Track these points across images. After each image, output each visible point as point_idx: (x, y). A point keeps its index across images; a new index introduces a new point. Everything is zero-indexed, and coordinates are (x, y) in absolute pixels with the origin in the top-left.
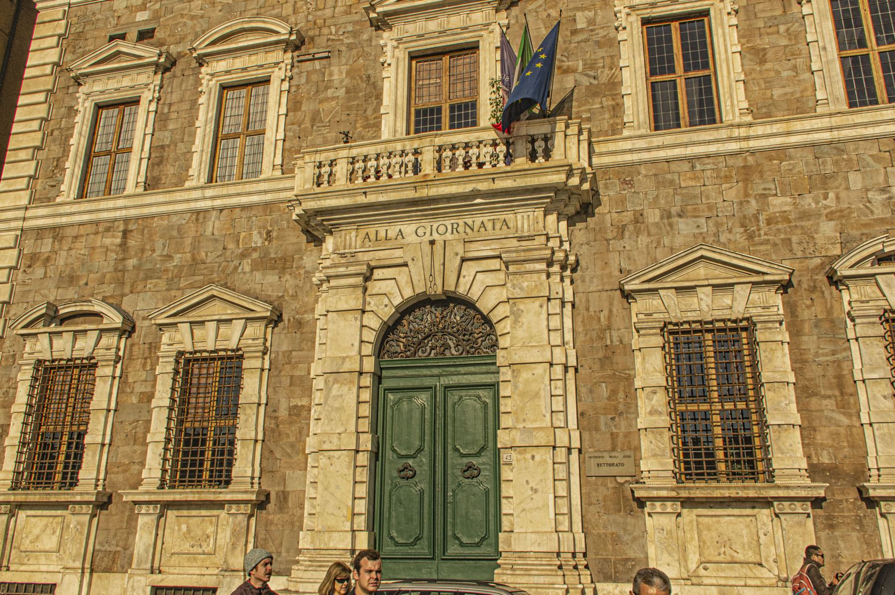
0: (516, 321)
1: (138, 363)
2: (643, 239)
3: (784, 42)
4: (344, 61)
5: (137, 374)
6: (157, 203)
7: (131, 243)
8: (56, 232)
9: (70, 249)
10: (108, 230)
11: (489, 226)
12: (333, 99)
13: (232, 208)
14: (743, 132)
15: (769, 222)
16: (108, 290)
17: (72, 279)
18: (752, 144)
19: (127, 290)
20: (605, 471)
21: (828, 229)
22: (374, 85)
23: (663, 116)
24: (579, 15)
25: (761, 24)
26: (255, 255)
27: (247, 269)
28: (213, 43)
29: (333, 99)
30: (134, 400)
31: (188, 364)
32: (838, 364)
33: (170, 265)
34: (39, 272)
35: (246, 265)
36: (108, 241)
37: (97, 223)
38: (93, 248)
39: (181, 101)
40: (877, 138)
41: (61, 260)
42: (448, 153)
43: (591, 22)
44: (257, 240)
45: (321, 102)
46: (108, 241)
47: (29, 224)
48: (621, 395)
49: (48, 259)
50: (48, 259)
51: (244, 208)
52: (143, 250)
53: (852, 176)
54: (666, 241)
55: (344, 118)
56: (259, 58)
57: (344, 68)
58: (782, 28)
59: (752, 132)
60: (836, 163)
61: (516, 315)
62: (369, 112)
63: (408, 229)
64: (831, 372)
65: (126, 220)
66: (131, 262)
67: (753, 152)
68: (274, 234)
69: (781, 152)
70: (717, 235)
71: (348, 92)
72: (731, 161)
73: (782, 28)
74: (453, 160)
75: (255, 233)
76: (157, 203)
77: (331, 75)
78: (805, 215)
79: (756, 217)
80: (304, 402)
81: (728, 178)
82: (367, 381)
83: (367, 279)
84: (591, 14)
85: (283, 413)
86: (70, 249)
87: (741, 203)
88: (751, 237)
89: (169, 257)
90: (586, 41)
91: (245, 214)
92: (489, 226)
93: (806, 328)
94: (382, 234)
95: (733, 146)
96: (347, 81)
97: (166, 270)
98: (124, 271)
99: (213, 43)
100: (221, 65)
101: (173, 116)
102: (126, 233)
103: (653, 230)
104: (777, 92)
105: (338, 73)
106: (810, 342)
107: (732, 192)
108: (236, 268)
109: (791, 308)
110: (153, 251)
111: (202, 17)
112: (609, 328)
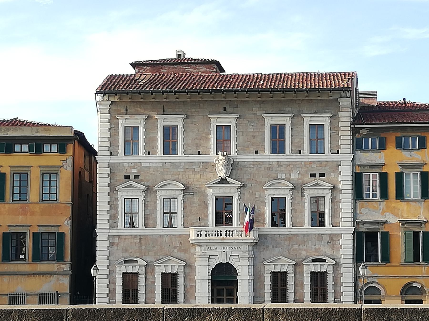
0: (241, 271)
1: (150, 274)
2: (268, 252)
3: (301, 208)
4: (197, 196)
5: (149, 276)
6: (148, 232)
7: (142, 242)
8: (119, 236)
9: (124, 242)
10: (135, 237)
11: (236, 248)
12: (195, 207)
13: (170, 235)
14: (290, 230)
15: (293, 250)
16: (138, 254)
17: (126, 251)
18: (291, 233)
19: (143, 255)
20: (258, 300)
21: (304, 253)
22: (206, 204)
23: (274, 224)
24: (257, 193)
25: (296, 202)
26: (178, 248)
27: (176, 251)
28: (161, 187)
29: (195, 207)
30: (150, 283)
31: (164, 275)
32: (302, 281)
33: (155, 249)
34: (115, 248)
35: (176, 250)
36: (135, 241)
37: (131, 235)
38: (131, 242)
39: (151, 201)
40: (315, 234)
41: (122, 245)
42: (228, 232)
43: (260, 196)
44: (178, 244)
45: (192, 207)
46: (135, 241)
47: (110, 234)
48: (262, 285)
49: (118, 244)
50: (118, 244)
51: (173, 235)
52: (146, 244)
53: (310, 242)
54: (273, 253)
55: (199, 213)
56: (173, 193)
57: (198, 198)
58: (301, 204)
59: (292, 230)
60: (307, 239)
61: (242, 269)
62: (205, 212)
63: (218, 247)
64: (301, 282)
65: (140, 235)
66: (143, 247)
67: (291, 234)
68: (182, 243)
69: (297, 235)
70: (283, 252)
71: (199, 205)
72: (287, 236)
73: (301, 204)
74: (229, 234)
75: (177, 242)
76: (148, 232)
77: (194, 199)
78: (300, 249)
79: (291, 249)
80: (194, 284)
81: (286, 240)
82: (210, 281)
83: (209, 258)
84: (260, 193)
85: (188, 287)
86: (124, 242)
87: (288, 245)
88: (289, 253)
89: (154, 247)
90: (258, 200)
91: (174, 237)
92: (236, 248)
93: (297, 273)
94: (212, 248)
95: (288, 233)
96: (199, 202)
97: (154, 250)
98: (141, 249)
99: (161, 187)
100: (163, 193)
101: (149, 205)
102: (140, 238)
103: (270, 250)
104: (298, 220)
105: (196, 199)
106: (298, 276)
107: (287, 243)
108: (173, 251)
109: (295, 269)
110: (149, 244)
111: (154, 174)
112: (260, 271)
